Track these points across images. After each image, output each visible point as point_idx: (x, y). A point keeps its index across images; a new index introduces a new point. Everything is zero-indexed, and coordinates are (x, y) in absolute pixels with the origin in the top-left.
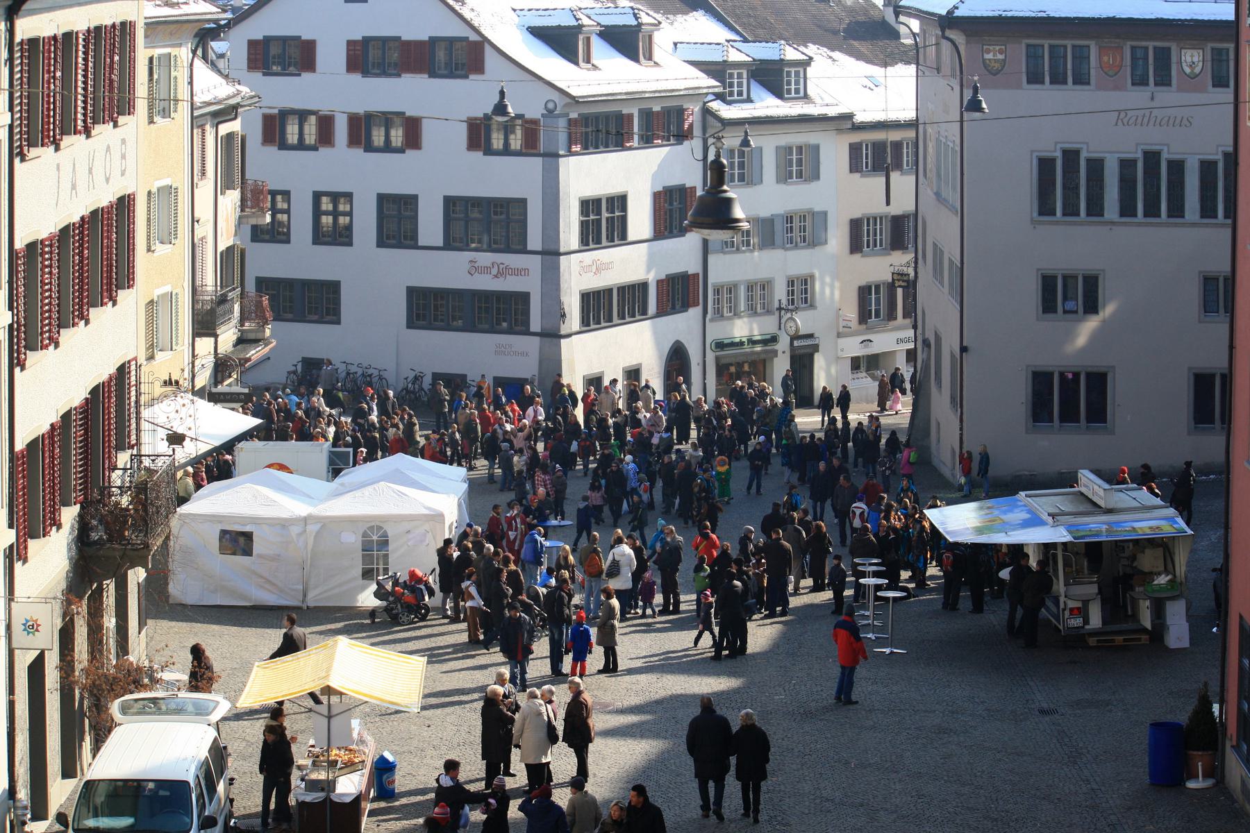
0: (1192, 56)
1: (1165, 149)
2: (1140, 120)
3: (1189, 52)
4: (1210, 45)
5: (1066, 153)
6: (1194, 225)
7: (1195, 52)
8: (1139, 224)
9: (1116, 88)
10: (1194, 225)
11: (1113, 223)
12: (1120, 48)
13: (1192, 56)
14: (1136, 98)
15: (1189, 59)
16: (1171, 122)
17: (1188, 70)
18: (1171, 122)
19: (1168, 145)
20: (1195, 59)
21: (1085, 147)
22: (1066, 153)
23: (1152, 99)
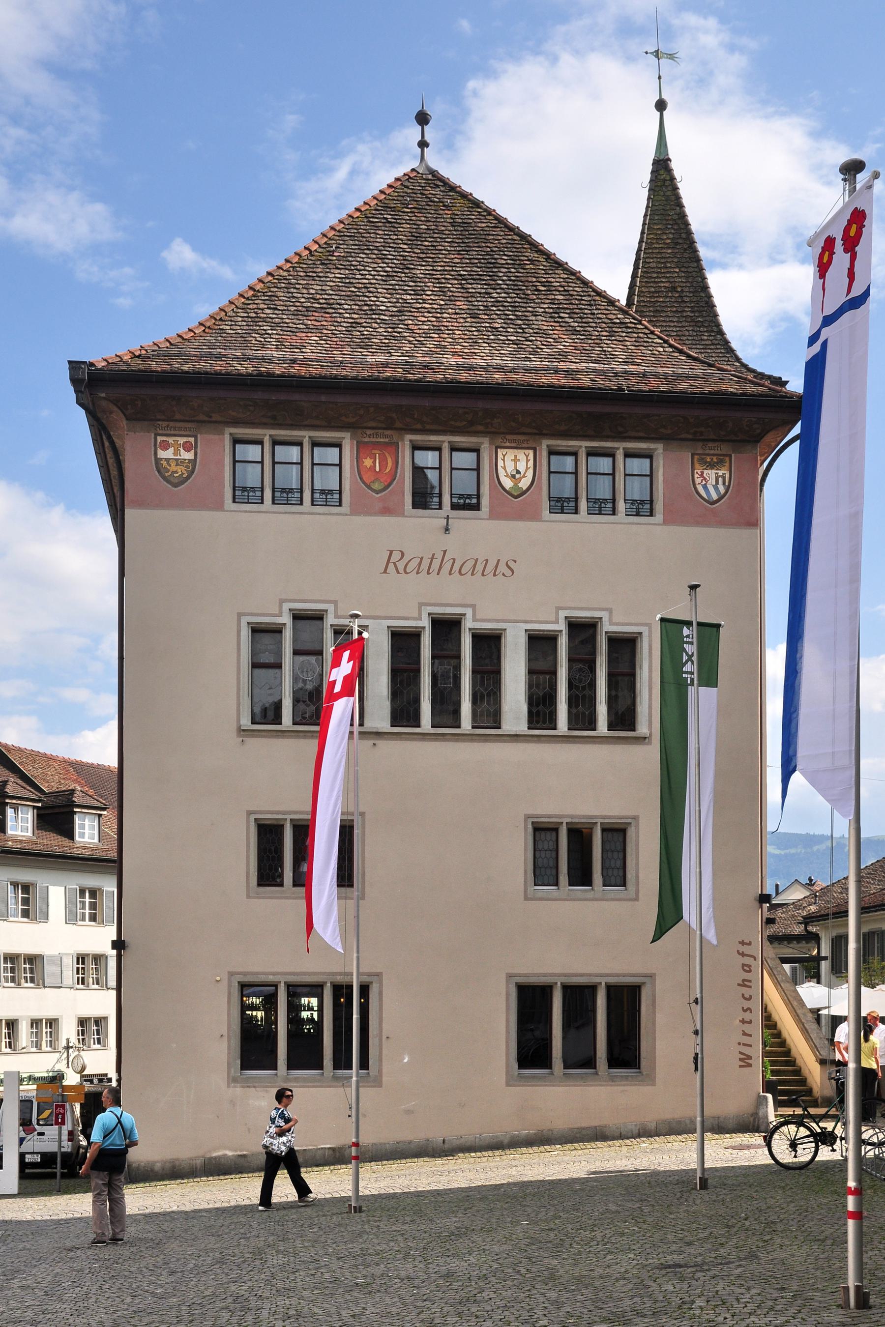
0: (516, 460)
1: (469, 612)
2: (425, 563)
3: (510, 454)
4: (545, 443)
5: (298, 617)
6: (516, 738)
7: (521, 454)
8: (425, 736)
9: (386, 511)
10: (516, 738)
11: (379, 735)
12: (394, 447)
13: (516, 460)
14: (417, 530)
15: (510, 468)
16: (480, 567)
17: (508, 483)
18: (480, 567)
19: (473, 607)
20: (521, 467)
21: (330, 608)
22: (298, 617)
23: (447, 529)
